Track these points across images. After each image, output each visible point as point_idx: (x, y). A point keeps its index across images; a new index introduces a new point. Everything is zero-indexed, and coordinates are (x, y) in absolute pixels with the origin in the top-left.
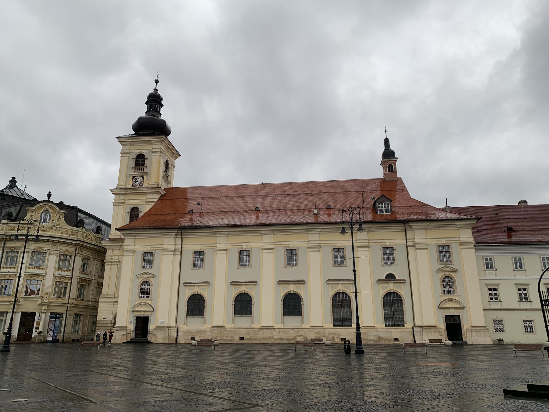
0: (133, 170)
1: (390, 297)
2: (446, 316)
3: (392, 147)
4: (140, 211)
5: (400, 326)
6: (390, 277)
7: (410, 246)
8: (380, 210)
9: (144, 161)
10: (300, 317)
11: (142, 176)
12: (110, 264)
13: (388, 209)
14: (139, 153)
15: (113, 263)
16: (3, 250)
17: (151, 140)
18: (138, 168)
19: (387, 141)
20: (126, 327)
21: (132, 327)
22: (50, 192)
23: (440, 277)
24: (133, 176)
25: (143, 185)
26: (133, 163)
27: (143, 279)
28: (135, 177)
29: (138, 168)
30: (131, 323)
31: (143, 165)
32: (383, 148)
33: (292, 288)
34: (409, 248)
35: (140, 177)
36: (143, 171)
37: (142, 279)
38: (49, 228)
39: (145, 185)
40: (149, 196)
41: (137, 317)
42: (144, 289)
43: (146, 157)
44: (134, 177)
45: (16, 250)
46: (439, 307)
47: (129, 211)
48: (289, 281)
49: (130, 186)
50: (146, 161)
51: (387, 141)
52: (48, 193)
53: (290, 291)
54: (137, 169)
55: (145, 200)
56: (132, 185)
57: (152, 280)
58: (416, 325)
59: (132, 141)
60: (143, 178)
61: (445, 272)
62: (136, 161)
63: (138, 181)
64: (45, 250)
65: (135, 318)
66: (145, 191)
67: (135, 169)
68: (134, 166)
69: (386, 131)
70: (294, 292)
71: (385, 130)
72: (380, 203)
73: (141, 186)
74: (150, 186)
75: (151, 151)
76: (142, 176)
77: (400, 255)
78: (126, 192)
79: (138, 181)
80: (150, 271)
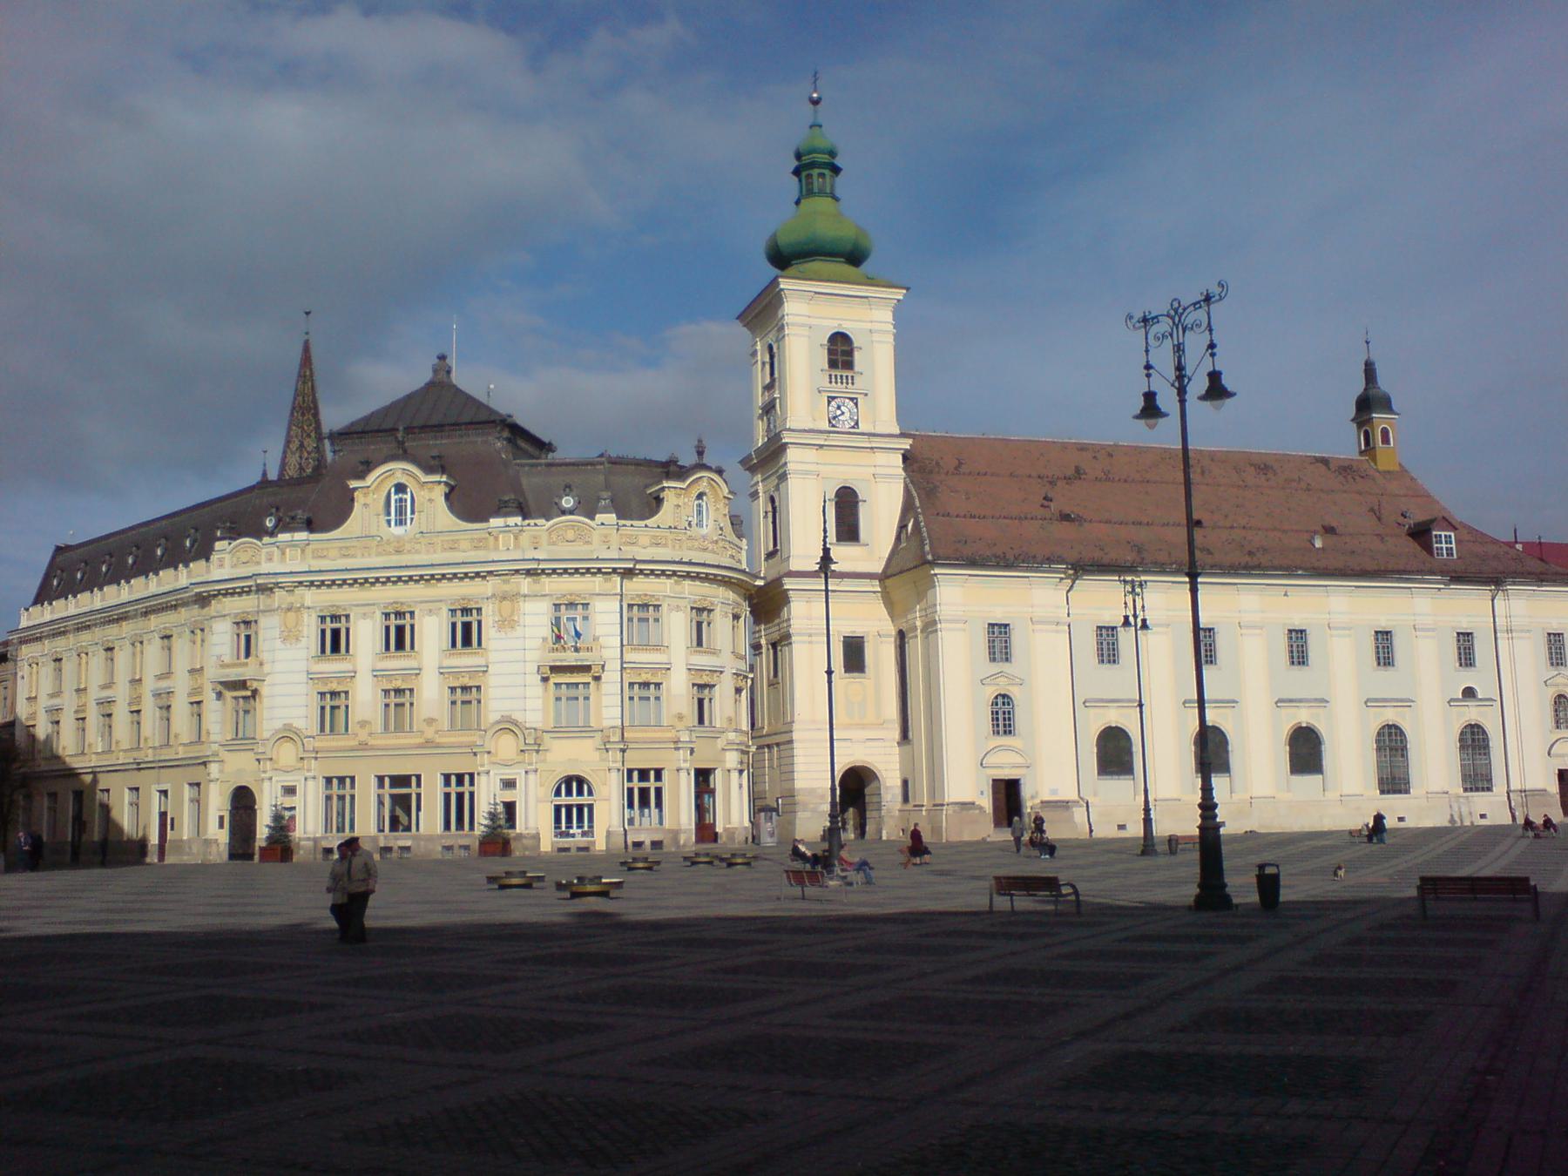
1: (1473, 733)
2: (1559, 770)
3: (1384, 383)
4: (860, 498)
5: (1483, 790)
6: (1469, 693)
7: (1502, 631)
8: (1437, 548)
9: (850, 353)
10: (1321, 776)
11: (852, 399)
12: (806, 638)
13: (1451, 548)
14: (836, 330)
15: (814, 638)
16: (621, 600)
18: (839, 374)
19: (1370, 371)
20: (973, 804)
21: (986, 802)
22: (700, 441)
23: (1551, 693)
24: (828, 397)
25: (857, 423)
26: (823, 358)
27: (998, 687)
28: (834, 398)
29: (839, 374)
30: (982, 793)
31: (849, 365)
32: (1359, 386)
33: (1304, 717)
34: (1498, 635)
35: (847, 400)
36: (853, 384)
37: (994, 688)
38: (716, 542)
39: (863, 427)
40: (881, 458)
41: (994, 780)
42: (997, 713)
43: (856, 344)
45: (656, 603)
46: (1549, 754)
48: (1301, 701)
49: (826, 426)
50: (857, 355)
51: (1370, 371)
52: (696, 443)
53: (1300, 723)
54: (841, 376)
55: (872, 470)
56: (830, 422)
57: (1014, 692)
58: (1512, 788)
59: (816, 293)
60: (856, 404)
61: (1557, 685)
62: (830, 352)
63: (843, 413)
64: (712, 604)
65: (991, 782)
66: (874, 445)
67: (830, 376)
68: (826, 366)
69: (1367, 343)
70: (1309, 725)
71: (1365, 339)
72: (1443, 534)
73: (853, 427)
74: (879, 430)
75: (869, 326)
76: (852, 399)
77: (1482, 650)
78: (822, 443)
79: (843, 413)
80: (1005, 667)
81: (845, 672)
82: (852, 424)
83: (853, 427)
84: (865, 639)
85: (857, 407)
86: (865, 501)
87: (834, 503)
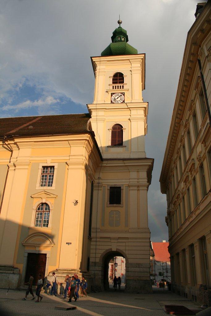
0: (111, 87)
9: (123, 79)
17: (129, 60)
24: (111, 93)
25: (124, 101)
28: (114, 94)
36: (123, 88)
40: (134, 112)
44: (112, 94)
47: (111, 128)
62: (113, 80)
67: (113, 87)
73: (122, 103)
81: (110, 203)
82: (122, 102)
83: (122, 103)
84: (122, 188)
85: (124, 96)
86: (125, 129)
87: (111, 131)
